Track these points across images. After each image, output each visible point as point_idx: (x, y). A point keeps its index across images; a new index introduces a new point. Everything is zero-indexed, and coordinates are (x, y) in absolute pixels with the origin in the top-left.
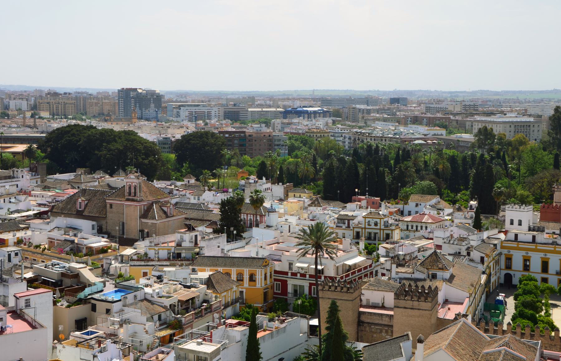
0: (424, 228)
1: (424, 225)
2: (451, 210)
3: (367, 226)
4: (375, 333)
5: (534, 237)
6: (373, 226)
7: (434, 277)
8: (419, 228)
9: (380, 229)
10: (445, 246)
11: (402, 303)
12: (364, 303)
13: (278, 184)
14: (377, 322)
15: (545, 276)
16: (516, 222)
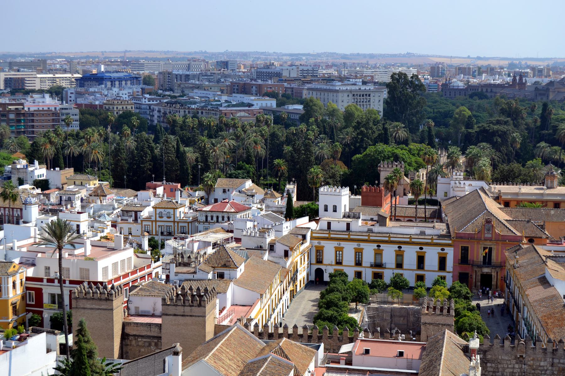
0: (226, 219)
1: (226, 216)
2: (262, 196)
3: (158, 219)
4: (143, 347)
5: (348, 225)
6: (165, 219)
7: (221, 276)
8: (220, 219)
9: (174, 222)
10: (243, 239)
11: (172, 310)
12: (133, 311)
13: (54, 169)
14: (144, 333)
15: (358, 269)
16: (330, 209)
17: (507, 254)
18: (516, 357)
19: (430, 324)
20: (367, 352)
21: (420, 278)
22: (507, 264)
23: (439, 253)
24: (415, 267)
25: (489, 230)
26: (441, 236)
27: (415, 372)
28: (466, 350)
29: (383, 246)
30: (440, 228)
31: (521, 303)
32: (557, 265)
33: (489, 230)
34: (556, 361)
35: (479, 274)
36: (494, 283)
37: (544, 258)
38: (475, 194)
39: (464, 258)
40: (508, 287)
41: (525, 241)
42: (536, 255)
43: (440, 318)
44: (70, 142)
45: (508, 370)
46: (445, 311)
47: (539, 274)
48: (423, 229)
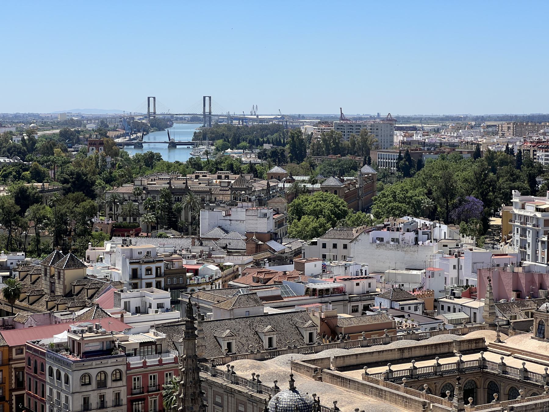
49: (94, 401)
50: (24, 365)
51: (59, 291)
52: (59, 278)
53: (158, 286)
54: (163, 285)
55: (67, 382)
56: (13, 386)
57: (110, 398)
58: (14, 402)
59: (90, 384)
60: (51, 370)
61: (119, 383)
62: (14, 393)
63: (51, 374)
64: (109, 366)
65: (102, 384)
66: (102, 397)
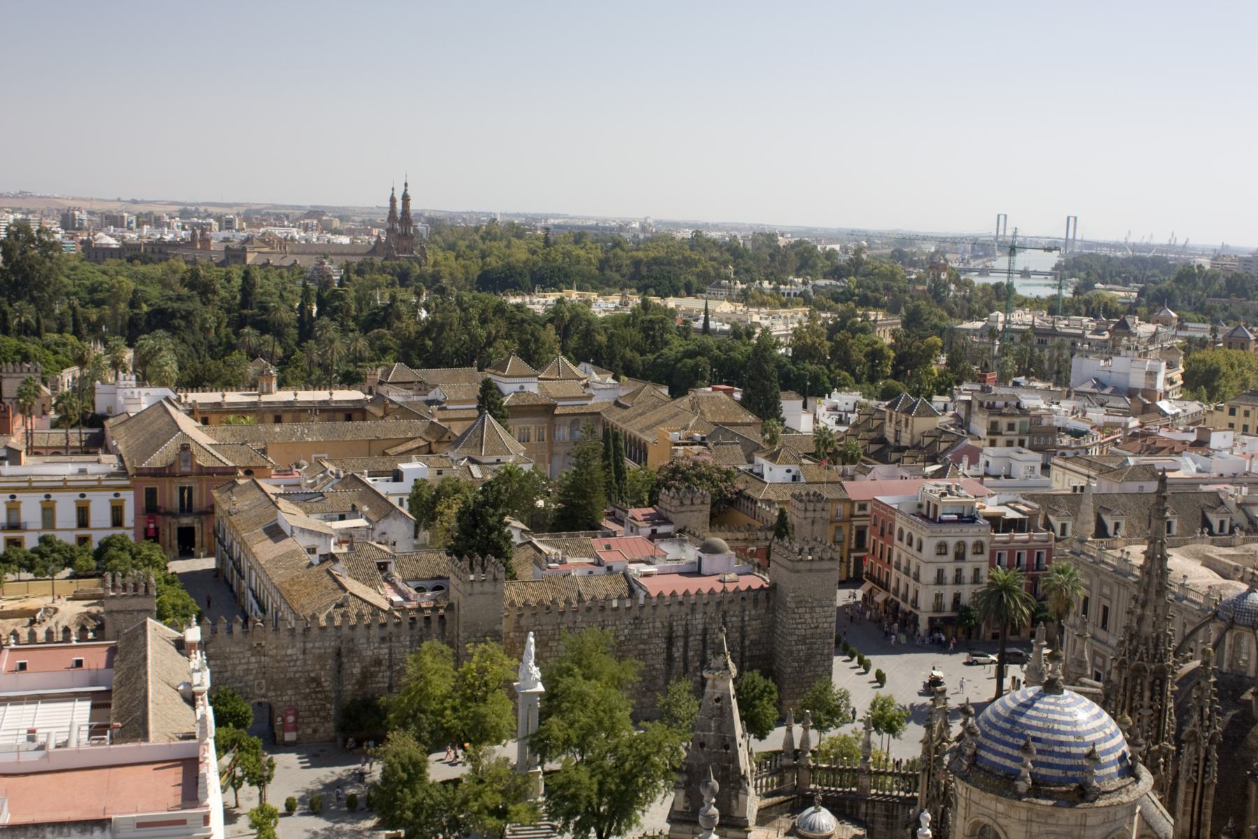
17: (216, 494)
18: (251, 646)
19: (118, 612)
20: (23, 667)
21: (83, 540)
22: (217, 510)
23: (111, 501)
24: (74, 525)
25: (186, 461)
26: (110, 475)
27: (103, 688)
28: (181, 645)
29: (20, 496)
30: (109, 462)
31: (245, 565)
32: (292, 506)
33: (186, 461)
34: (309, 645)
35: (175, 527)
36: (197, 539)
37: (273, 498)
38: (159, 406)
39: (150, 507)
40: (221, 542)
41: (241, 473)
42: (260, 494)
43: (134, 601)
44: (1236, 383)
45: (240, 668)
46: (141, 591)
47: (268, 522)
48: (83, 466)
49: (950, 574)
50: (868, 523)
51: (905, 440)
52: (907, 426)
53: (1021, 443)
54: (1027, 443)
55: (920, 549)
56: (853, 546)
57: (968, 573)
58: (852, 564)
59: (946, 554)
60: (901, 531)
61: (979, 557)
62: (853, 555)
63: (901, 539)
64: (970, 535)
65: (960, 556)
66: (959, 571)
